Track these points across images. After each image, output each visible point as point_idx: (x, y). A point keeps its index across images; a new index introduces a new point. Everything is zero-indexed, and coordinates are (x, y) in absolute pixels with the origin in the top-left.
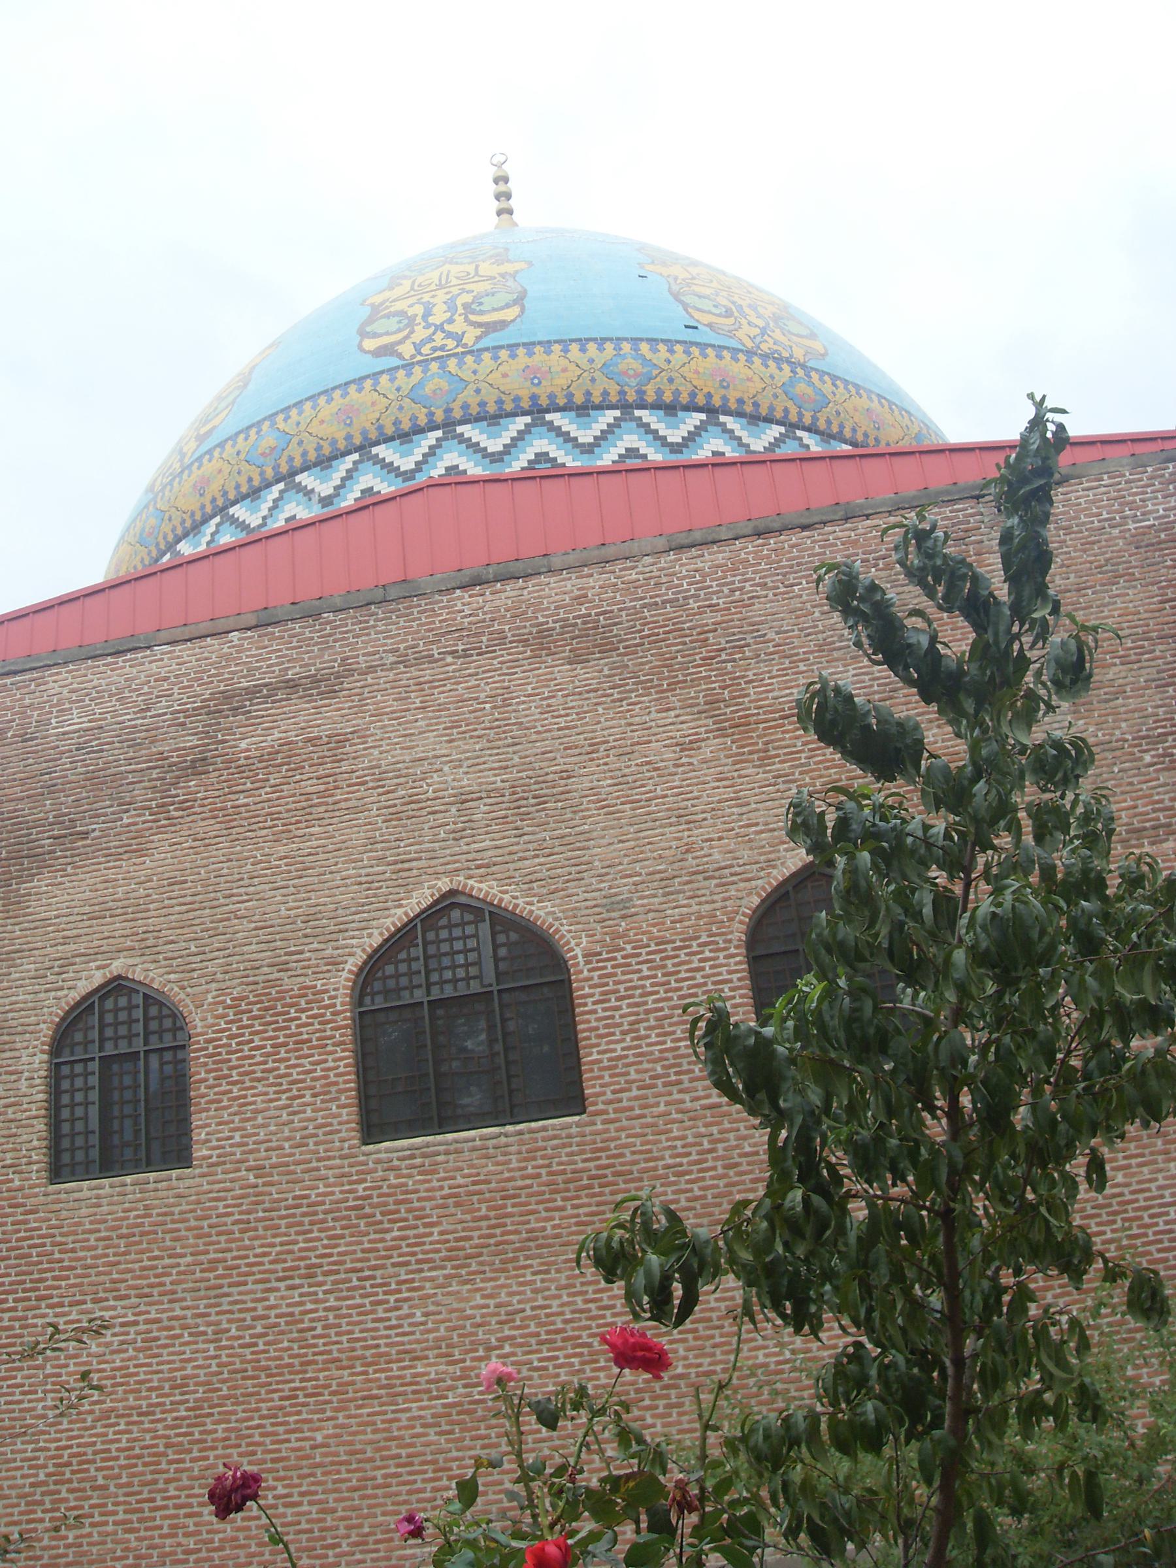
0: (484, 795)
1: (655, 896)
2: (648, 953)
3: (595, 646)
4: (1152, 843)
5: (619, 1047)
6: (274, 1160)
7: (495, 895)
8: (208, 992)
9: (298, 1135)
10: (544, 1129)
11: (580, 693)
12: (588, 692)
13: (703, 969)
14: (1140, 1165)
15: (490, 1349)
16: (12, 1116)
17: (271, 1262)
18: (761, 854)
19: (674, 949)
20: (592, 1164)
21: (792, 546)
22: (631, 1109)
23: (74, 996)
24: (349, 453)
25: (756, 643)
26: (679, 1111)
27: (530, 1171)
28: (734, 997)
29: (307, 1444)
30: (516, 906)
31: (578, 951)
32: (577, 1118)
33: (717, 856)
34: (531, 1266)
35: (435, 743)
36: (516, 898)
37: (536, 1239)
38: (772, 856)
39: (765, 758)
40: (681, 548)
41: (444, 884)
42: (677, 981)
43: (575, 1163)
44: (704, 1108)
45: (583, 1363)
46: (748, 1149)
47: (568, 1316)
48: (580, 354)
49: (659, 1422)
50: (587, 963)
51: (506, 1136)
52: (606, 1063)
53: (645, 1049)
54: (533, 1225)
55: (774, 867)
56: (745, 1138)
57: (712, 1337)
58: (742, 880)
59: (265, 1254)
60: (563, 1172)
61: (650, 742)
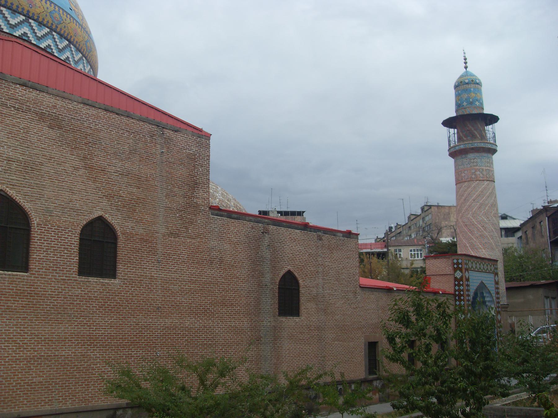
0: (16, 161)
1: (59, 212)
2: (55, 229)
3: (57, 125)
4: (174, 238)
5: (42, 255)
7: (14, 196)
10: (17, 275)
11: (50, 139)
12: (52, 139)
13: (68, 238)
14: (155, 318)
18: (89, 209)
19: (62, 230)
20: (29, 289)
21: (113, 118)
22: (42, 275)
25: (99, 144)
26: (55, 279)
27: (11, 287)
28: (74, 249)
30: (20, 202)
31: (35, 222)
33: (77, 206)
34: (6, 317)
35: (3, 136)
36: (20, 199)
37: (9, 309)
38: (92, 211)
39: (95, 181)
40: (85, 104)
42: (61, 240)
43: (24, 288)
44: (61, 279)
45: (16, 349)
46: (70, 294)
47: (15, 334)
48: (45, 4)
49: (34, 368)
50: (37, 227)
51: (5, 275)
52: (38, 259)
53: (49, 258)
54: (9, 305)
55: (91, 214)
56: (70, 291)
57: (52, 346)
58: (83, 215)
60: (20, 290)
61: (66, 163)
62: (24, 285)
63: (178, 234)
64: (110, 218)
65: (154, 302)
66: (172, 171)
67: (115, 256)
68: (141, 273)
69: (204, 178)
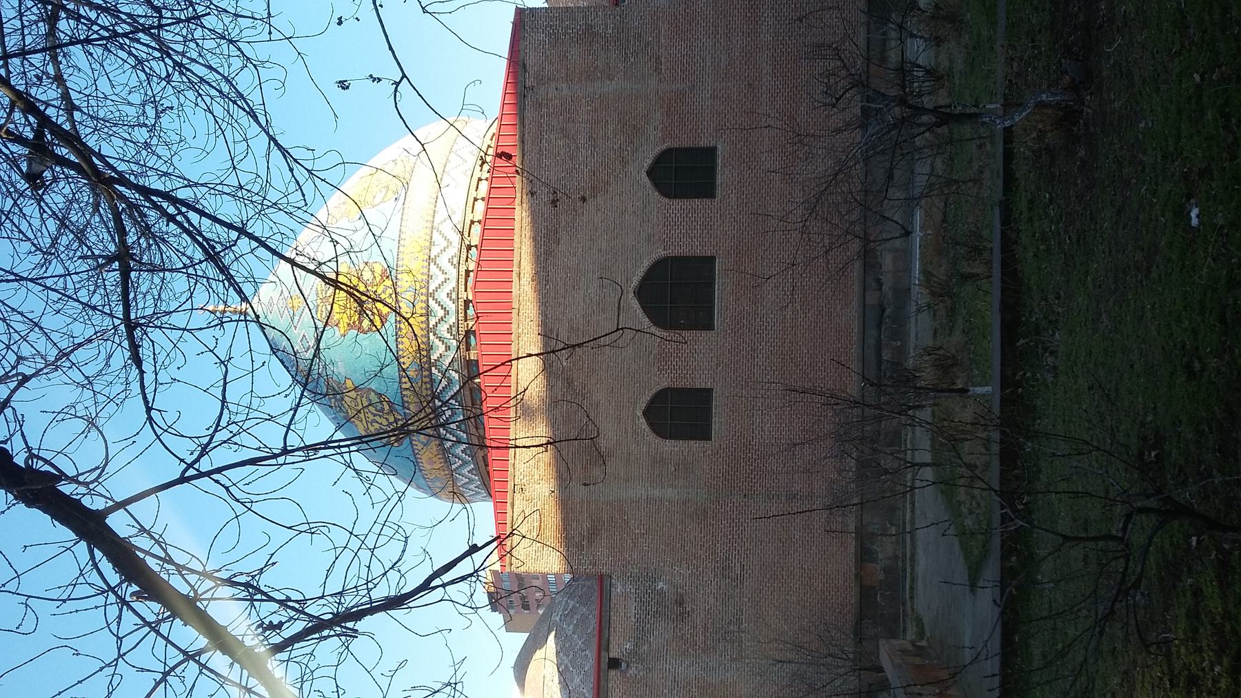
1: (648, 226)
6: (715, 360)
8: (654, 380)
9: (708, 351)
10: (719, 270)
14: (762, 89)
15: (785, 294)
16: (686, 454)
17: (748, 363)
23: (648, 429)
24: (429, 337)
26: (721, 226)
29: (807, 355)
31: (662, 253)
32: (717, 260)
41: (631, 295)
44: (720, 218)
59: (746, 364)
62: (728, 262)
63: (656, 59)
64: (648, 160)
65: (742, 92)
66: (577, 71)
67: (691, 149)
68: (708, 113)
69: (578, 15)
